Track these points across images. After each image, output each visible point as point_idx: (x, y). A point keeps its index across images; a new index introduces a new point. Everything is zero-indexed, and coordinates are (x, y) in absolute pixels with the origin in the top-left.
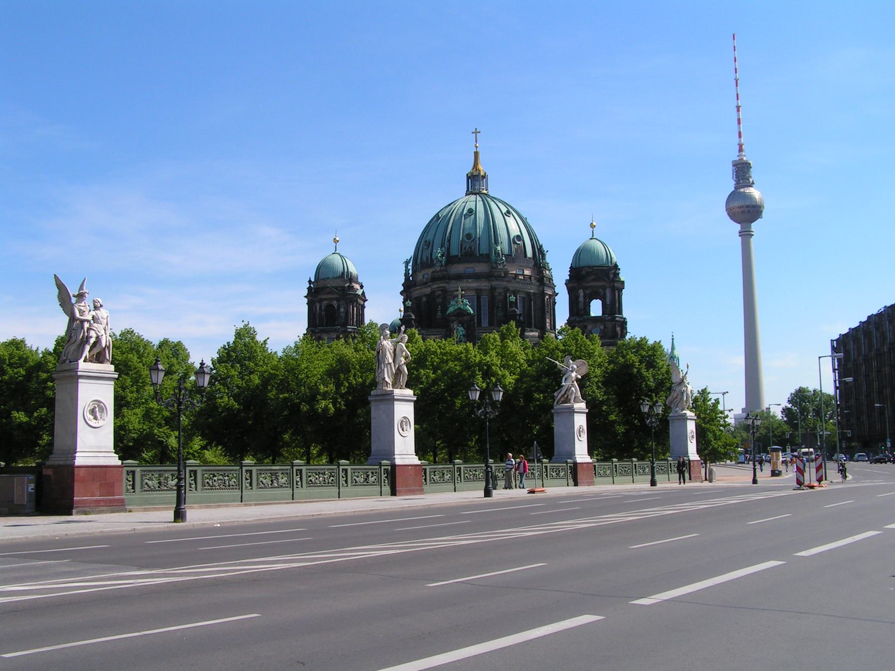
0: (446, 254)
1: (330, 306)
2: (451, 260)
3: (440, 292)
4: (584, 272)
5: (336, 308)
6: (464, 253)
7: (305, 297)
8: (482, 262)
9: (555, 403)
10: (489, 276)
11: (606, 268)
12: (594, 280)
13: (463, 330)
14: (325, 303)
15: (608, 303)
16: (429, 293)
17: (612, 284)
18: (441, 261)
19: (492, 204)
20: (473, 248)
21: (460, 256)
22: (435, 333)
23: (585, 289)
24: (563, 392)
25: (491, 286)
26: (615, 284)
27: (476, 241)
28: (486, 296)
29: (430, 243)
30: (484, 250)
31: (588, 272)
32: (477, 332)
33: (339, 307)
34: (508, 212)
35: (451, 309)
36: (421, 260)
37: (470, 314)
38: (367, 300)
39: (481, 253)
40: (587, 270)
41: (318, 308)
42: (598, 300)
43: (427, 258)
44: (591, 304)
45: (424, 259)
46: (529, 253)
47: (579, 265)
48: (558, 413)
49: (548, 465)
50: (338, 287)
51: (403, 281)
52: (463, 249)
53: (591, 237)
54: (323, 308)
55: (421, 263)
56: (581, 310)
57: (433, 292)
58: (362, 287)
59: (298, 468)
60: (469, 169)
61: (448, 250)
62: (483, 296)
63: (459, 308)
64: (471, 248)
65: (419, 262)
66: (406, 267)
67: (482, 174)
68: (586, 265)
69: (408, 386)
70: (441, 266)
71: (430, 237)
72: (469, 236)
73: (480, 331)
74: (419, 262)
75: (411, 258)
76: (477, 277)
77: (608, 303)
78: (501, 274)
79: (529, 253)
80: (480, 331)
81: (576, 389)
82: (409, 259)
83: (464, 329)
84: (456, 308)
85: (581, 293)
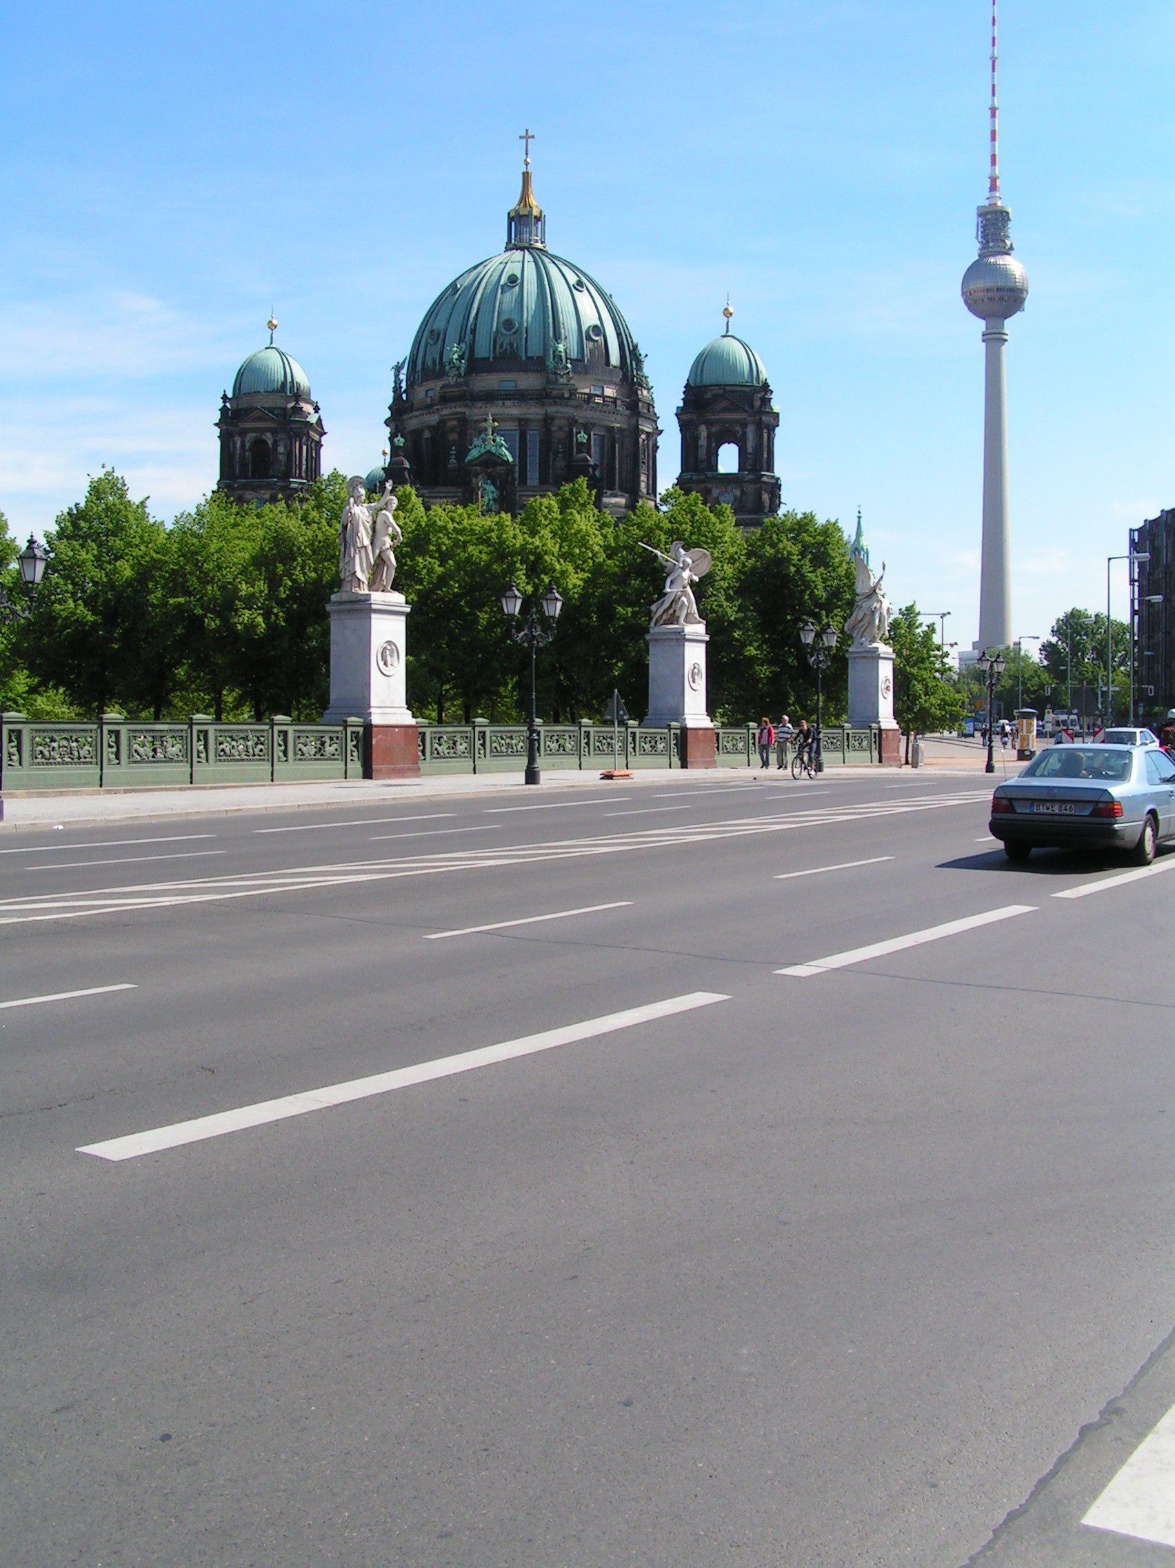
0: (467, 354)
1: (260, 442)
2: (475, 365)
5: (271, 446)
7: (216, 425)
8: (533, 371)
9: (652, 624)
10: (541, 397)
11: (748, 389)
12: (726, 410)
13: (493, 489)
14: (250, 437)
15: (750, 450)
16: (434, 423)
18: (459, 368)
19: (552, 268)
20: (515, 345)
21: (491, 359)
23: (709, 424)
24: (666, 605)
25: (546, 413)
26: (763, 418)
27: (521, 334)
28: (535, 432)
29: (439, 335)
30: (535, 350)
32: (518, 494)
33: (275, 444)
34: (580, 283)
35: (474, 453)
36: (423, 363)
38: (325, 433)
39: (530, 354)
41: (238, 445)
42: (732, 445)
43: (434, 362)
45: (429, 363)
46: (615, 359)
47: (701, 381)
48: (656, 640)
49: (637, 731)
50: (276, 408)
51: (390, 401)
53: (724, 333)
54: (248, 445)
55: (423, 369)
57: (442, 422)
58: (317, 409)
59: (200, 727)
60: (512, 203)
61: (472, 349)
64: (511, 345)
65: (419, 367)
66: (397, 376)
67: (535, 212)
68: (714, 382)
69: (396, 587)
70: (459, 376)
71: (439, 324)
73: (524, 493)
74: (419, 367)
75: (404, 362)
76: (520, 396)
77: (750, 450)
78: (563, 394)
79: (615, 359)
80: (524, 493)
81: (689, 600)
82: (401, 362)
84: (483, 451)
85: (703, 431)
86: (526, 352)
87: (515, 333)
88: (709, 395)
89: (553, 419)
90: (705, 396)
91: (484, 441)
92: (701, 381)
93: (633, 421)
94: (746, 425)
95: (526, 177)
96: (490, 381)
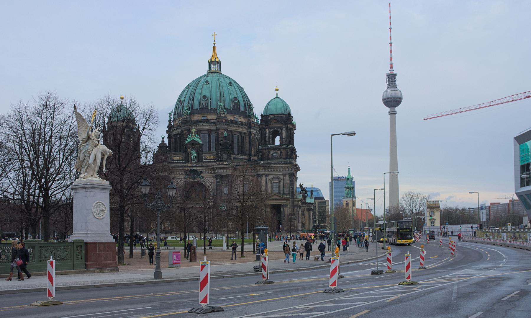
0: (191, 108)
2: (193, 111)
3: (186, 131)
4: (269, 118)
6: (202, 107)
8: (213, 113)
10: (216, 122)
11: (283, 116)
12: (275, 123)
13: (195, 153)
15: (284, 137)
17: (286, 126)
20: (207, 104)
22: (178, 155)
23: (270, 128)
26: (288, 126)
27: (209, 100)
28: (214, 134)
29: (182, 102)
30: (214, 106)
31: (272, 118)
32: (204, 154)
35: (189, 140)
36: (178, 112)
37: (199, 144)
39: (212, 107)
40: (271, 117)
43: (181, 110)
44: (276, 139)
47: (267, 114)
51: (168, 124)
52: (201, 105)
55: (177, 113)
56: (267, 142)
57: (182, 131)
60: (209, 56)
61: (192, 106)
62: (213, 134)
63: (193, 140)
64: (206, 104)
66: (170, 116)
67: (217, 60)
70: (187, 115)
72: (205, 97)
73: (206, 154)
77: (284, 137)
78: (223, 121)
80: (206, 154)
83: (196, 152)
84: (191, 140)
86: (210, 106)
87: (206, 100)
88: (269, 118)
89: (219, 129)
90: (268, 119)
91: (192, 136)
92: (267, 114)
93: (249, 130)
94: (282, 128)
95: (214, 48)
96: (199, 117)
